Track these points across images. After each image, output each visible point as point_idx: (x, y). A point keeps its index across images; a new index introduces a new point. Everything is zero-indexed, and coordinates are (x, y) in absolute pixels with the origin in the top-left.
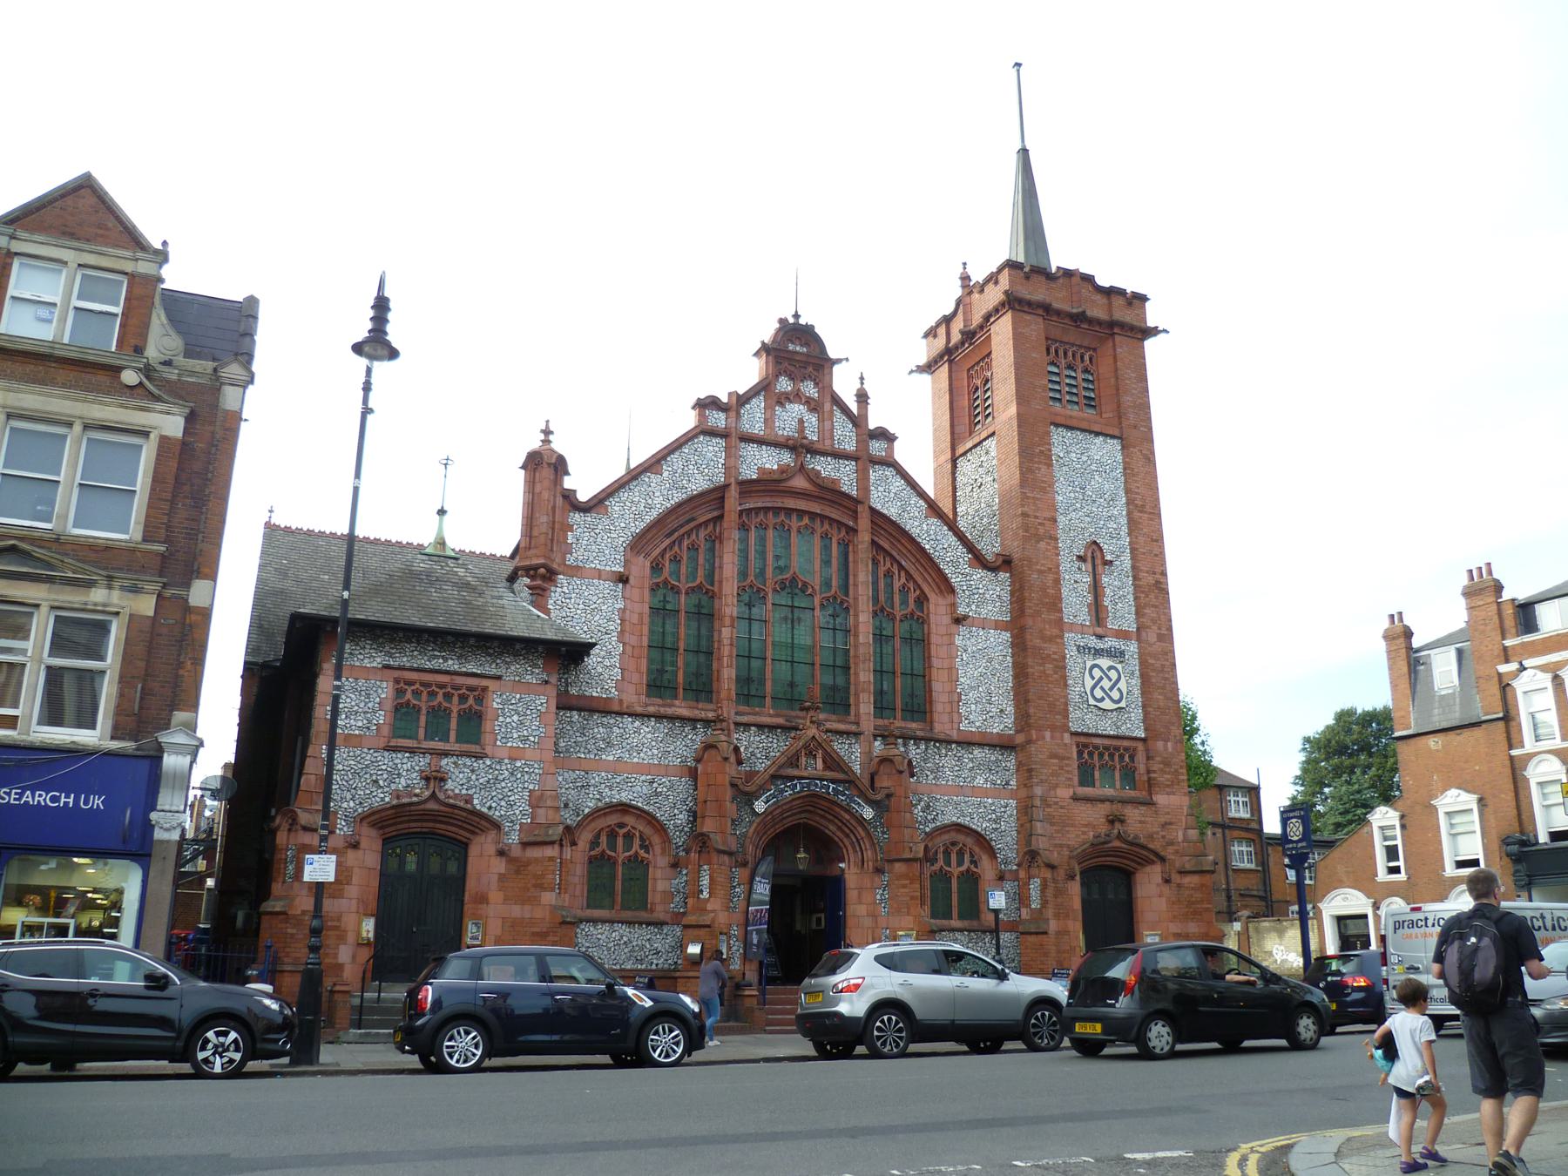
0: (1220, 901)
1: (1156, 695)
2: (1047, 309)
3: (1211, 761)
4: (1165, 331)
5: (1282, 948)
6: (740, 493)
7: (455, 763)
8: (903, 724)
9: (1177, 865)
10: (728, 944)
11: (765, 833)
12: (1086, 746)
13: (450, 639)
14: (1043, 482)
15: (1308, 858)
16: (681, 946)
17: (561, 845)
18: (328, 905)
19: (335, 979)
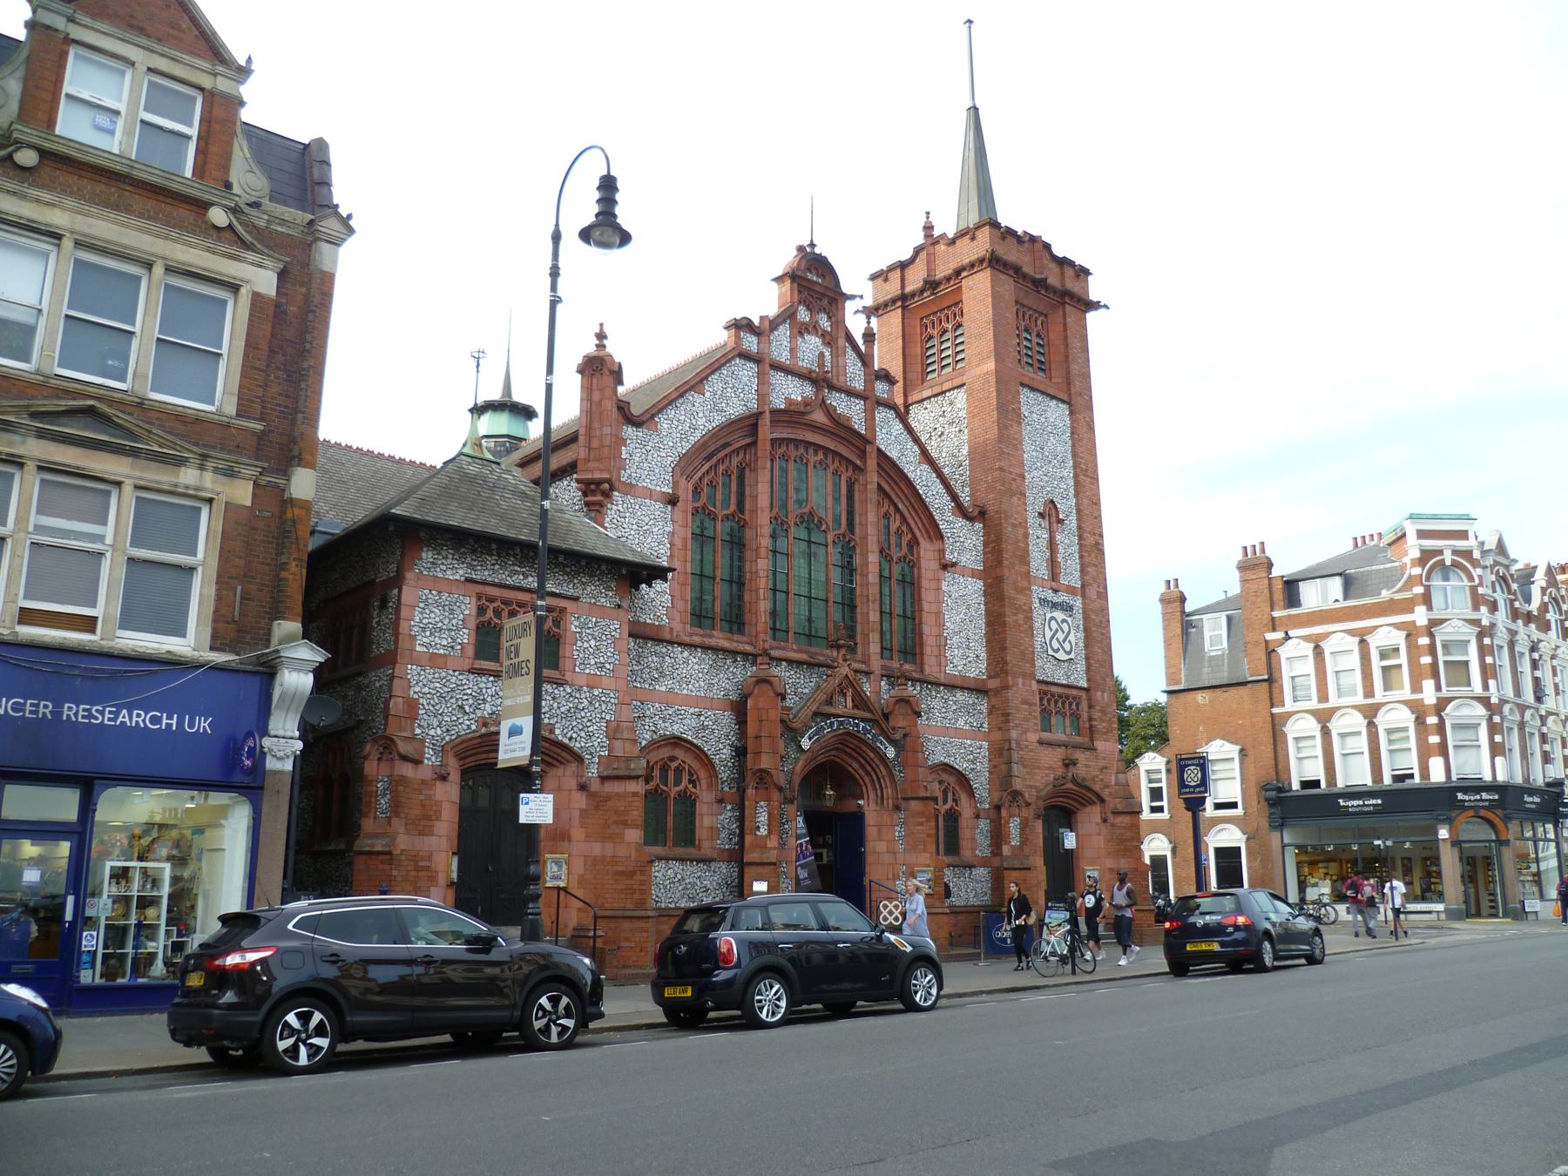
2: (1015, 271)
4: (1106, 306)
6: (771, 422)
9: (1111, 805)
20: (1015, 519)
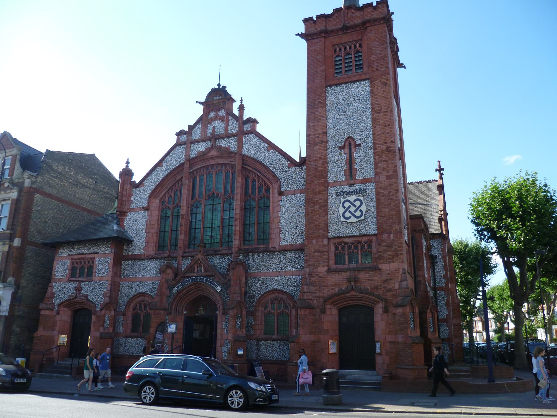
14: (319, 116)
20: (317, 157)
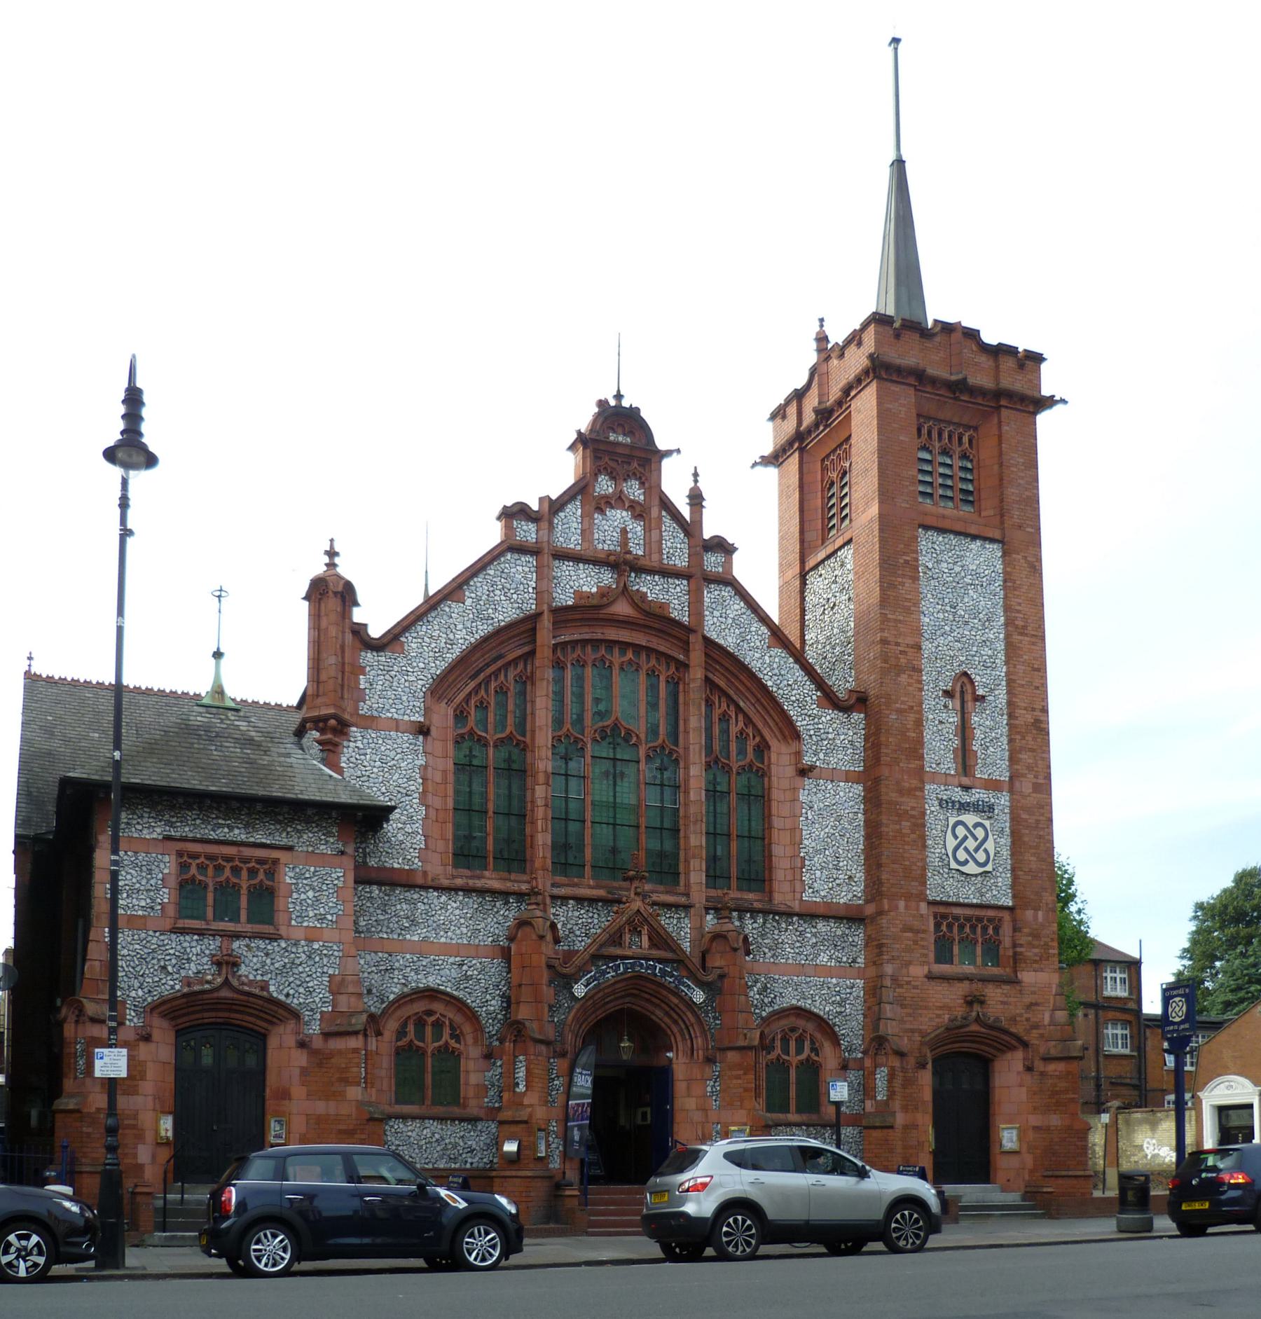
0: (1088, 1090)
1: (1028, 857)
3: (1087, 932)
5: (1154, 1141)
7: (247, 946)
8: (738, 895)
10: (547, 1141)
11: (586, 1019)
12: (944, 916)
13: (235, 804)
15: (1190, 1041)
16: (497, 1143)
17: (366, 1036)
18: (122, 1102)
19: (135, 1181)
